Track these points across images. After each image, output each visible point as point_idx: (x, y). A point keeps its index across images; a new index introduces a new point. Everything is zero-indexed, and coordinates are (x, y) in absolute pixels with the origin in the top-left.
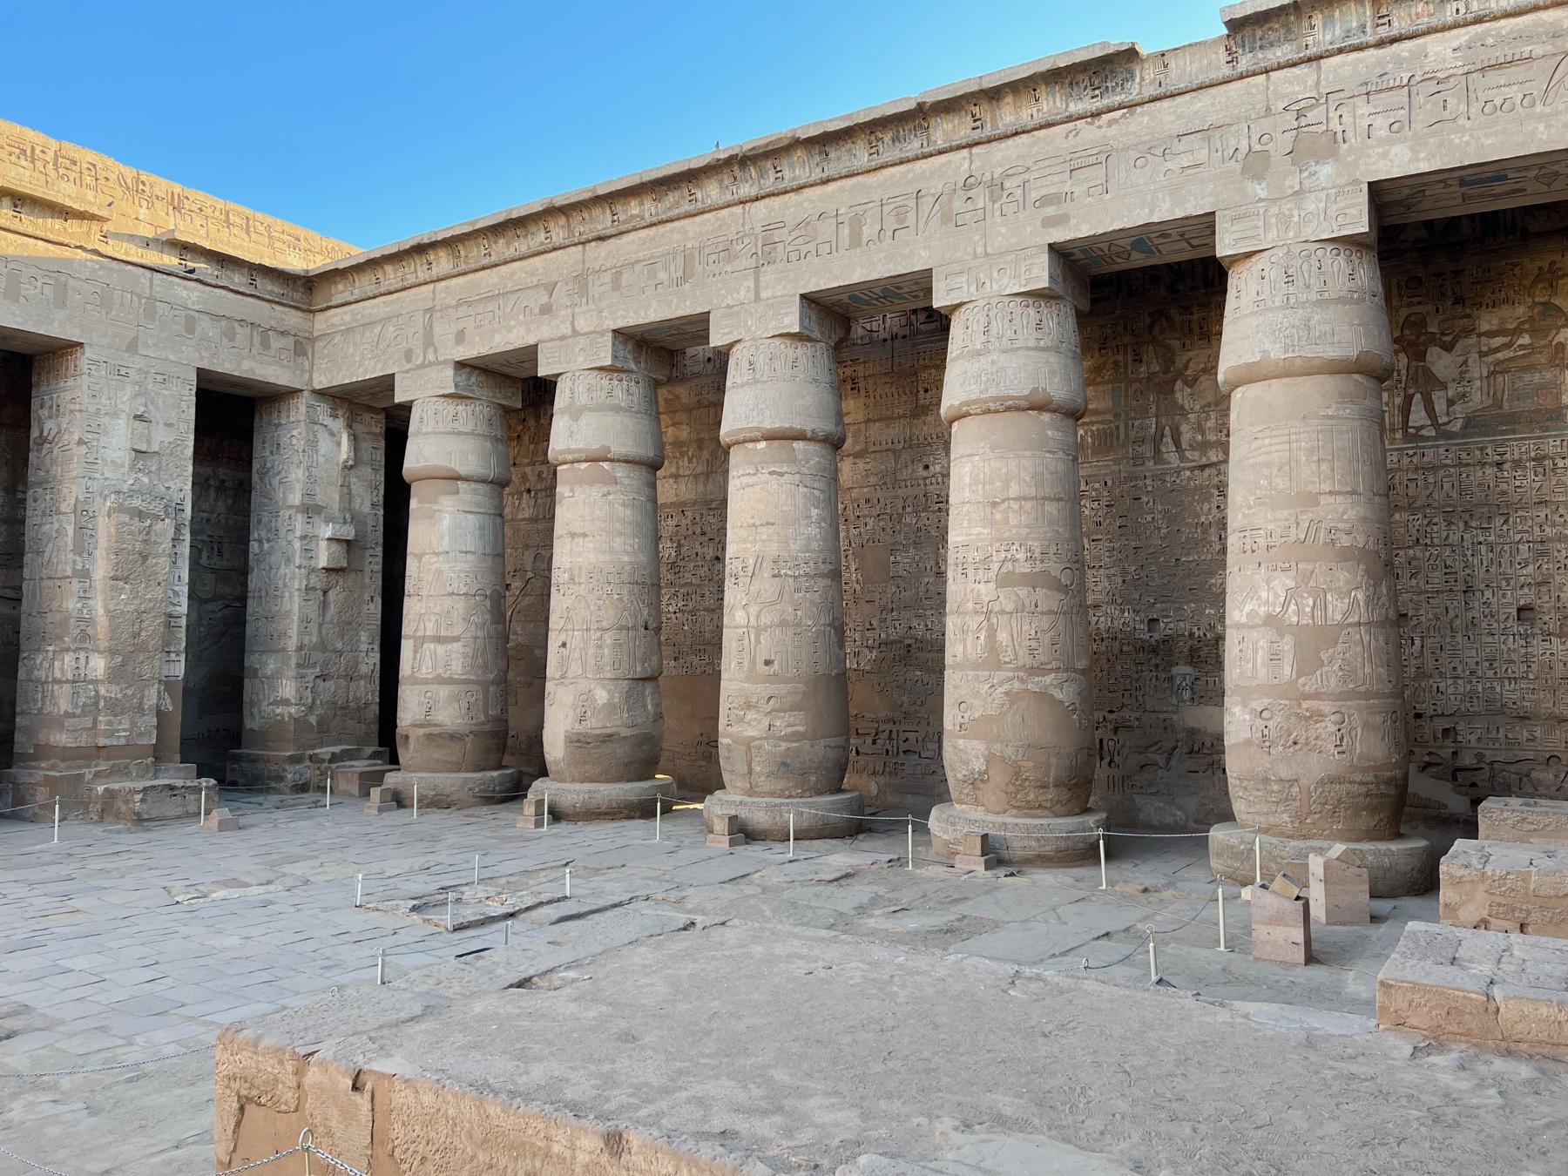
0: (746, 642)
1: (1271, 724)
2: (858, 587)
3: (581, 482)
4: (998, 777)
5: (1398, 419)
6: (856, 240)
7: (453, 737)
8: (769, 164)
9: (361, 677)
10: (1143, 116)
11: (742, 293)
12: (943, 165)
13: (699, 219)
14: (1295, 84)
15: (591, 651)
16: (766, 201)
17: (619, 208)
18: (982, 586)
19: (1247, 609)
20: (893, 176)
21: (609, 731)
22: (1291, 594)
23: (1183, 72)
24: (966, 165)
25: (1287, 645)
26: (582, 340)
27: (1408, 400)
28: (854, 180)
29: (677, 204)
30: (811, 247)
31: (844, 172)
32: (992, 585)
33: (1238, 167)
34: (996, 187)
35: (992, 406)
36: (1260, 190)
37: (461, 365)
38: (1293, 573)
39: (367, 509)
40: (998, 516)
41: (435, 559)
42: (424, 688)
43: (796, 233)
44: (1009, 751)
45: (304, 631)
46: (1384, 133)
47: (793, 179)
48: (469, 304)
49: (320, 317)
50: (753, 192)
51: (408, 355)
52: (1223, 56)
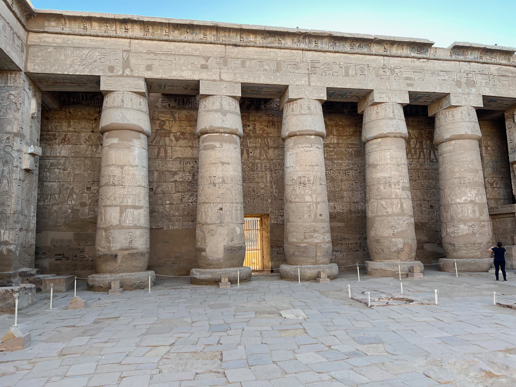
0: (312, 208)
1: (475, 229)
2: (276, 194)
3: (226, 142)
4: (407, 250)
5: (428, 156)
6: (347, 75)
7: (142, 254)
8: (313, 40)
9: (31, 231)
10: (431, 63)
11: (303, 82)
12: (375, 59)
13: (283, 50)
14: (465, 66)
15: (234, 212)
16: (312, 52)
17: (244, 36)
18: (397, 190)
19: (464, 198)
20: (359, 57)
21: (241, 245)
22: (477, 195)
23: (440, 54)
24: (383, 61)
25: (477, 208)
26: (225, 84)
27: (430, 152)
28: (345, 55)
29: (273, 43)
30: (331, 72)
31: (343, 51)
32: (400, 190)
33: (455, 83)
34: (392, 71)
35: (398, 135)
36: (460, 90)
37: (146, 80)
38: (476, 189)
39: (36, 141)
40: (400, 169)
41: (132, 168)
42: (128, 231)
43: (324, 66)
44: (410, 241)
45: (17, 204)
46: (484, 84)
47: (322, 48)
48: (156, 54)
49: (31, 35)
50: (306, 47)
51: (111, 69)
52: (449, 54)
